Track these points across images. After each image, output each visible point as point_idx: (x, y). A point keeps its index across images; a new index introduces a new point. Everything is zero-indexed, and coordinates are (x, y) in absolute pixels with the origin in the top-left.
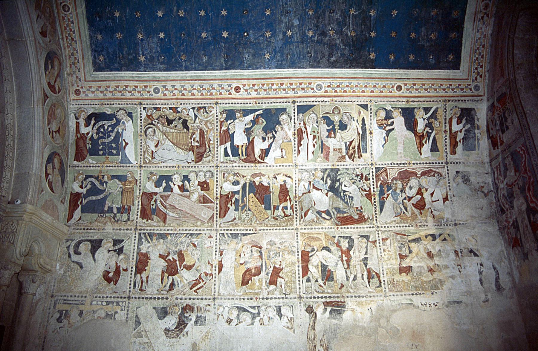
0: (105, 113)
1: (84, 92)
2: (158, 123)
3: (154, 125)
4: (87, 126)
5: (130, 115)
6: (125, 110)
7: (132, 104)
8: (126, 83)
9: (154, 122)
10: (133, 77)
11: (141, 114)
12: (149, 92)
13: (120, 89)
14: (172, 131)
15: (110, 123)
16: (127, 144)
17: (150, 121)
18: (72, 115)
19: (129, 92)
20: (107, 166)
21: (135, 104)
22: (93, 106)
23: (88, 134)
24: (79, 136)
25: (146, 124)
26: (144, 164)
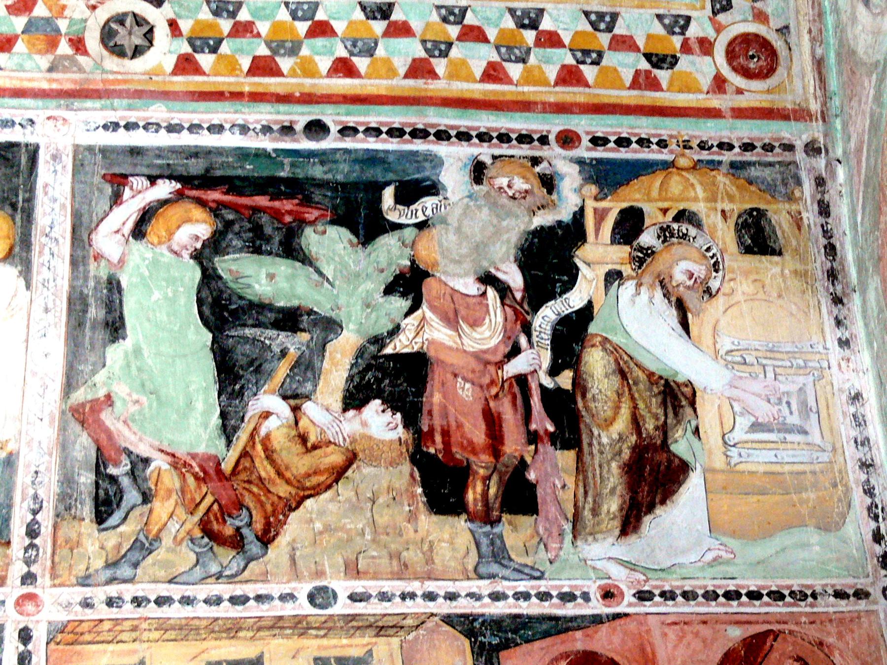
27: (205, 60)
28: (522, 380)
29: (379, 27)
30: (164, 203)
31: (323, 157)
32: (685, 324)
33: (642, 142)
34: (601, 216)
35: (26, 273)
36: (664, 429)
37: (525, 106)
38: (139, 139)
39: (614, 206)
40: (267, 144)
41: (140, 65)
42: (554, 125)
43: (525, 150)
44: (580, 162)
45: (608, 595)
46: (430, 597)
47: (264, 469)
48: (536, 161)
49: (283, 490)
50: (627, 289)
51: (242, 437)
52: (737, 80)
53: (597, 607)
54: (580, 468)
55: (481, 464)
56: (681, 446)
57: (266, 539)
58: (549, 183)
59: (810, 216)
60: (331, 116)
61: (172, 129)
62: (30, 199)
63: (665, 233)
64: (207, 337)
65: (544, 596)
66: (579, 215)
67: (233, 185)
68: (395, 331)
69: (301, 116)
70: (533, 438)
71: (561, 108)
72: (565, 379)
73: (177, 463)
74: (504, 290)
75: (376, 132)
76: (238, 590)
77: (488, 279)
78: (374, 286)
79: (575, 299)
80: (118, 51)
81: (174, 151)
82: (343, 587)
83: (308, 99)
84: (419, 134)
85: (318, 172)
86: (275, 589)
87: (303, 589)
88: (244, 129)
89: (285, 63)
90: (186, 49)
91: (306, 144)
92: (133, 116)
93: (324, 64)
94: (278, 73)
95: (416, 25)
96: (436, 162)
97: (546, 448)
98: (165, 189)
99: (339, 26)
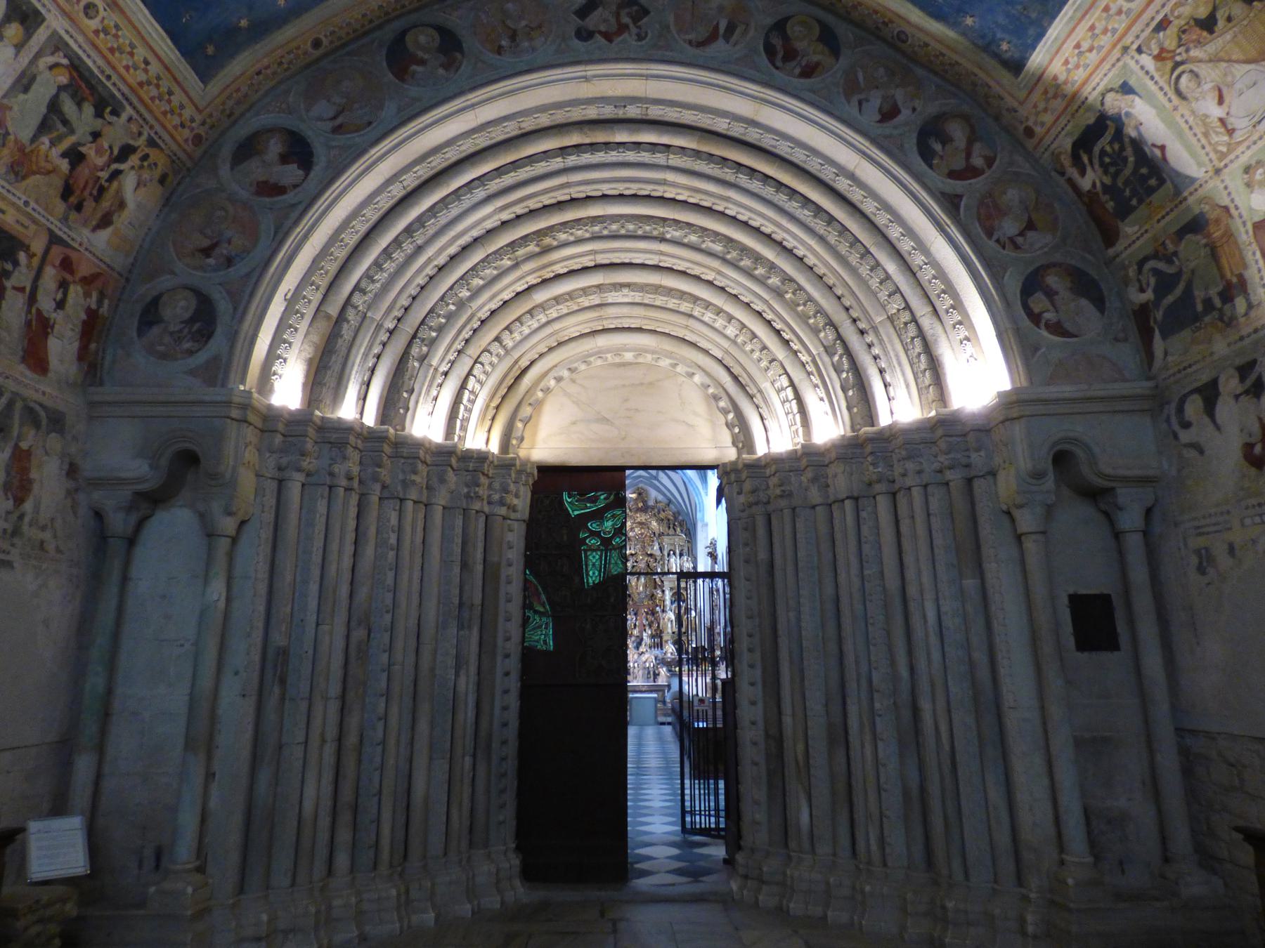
0: (1088, 127)
1: (1036, 123)
2: (1187, 51)
3: (1182, 63)
4: (1083, 173)
5: (1126, 89)
6: (1111, 90)
7: (1113, 65)
8: (1071, 43)
9: (1178, 58)
10: (1071, 18)
11: (1142, 68)
12: (1120, 12)
13: (1073, 61)
14: (1228, 37)
15: (1108, 136)
16: (1163, 148)
17: (1170, 64)
18: (1053, 174)
19: (1090, 50)
20: (1159, 221)
21: (1118, 60)
22: (1063, 133)
23: (1094, 185)
24: (1086, 199)
25: (1167, 76)
26: (1220, 160)
27: (102, 35)
28: (99, 178)
29: (143, 66)
30: (63, 65)
31: (105, 87)
32: (136, 189)
33: (163, 141)
34: (143, 150)
35: (16, 55)
36: (114, 211)
37: (150, 111)
38: (71, 42)
39: (147, 150)
40: (96, 71)
41: (86, 21)
42: (152, 122)
43: (141, 122)
44: (149, 135)
45: (80, 245)
46: (48, 220)
47: (34, 159)
48: (142, 127)
49: (34, 168)
50: (133, 172)
51: (34, 146)
52: (190, 142)
53: (76, 245)
54: (95, 209)
55: (78, 193)
56: (115, 218)
57: (24, 178)
58: (140, 134)
59: (175, 183)
60: (114, 78)
61: (80, 47)
62: (33, 33)
63: (149, 166)
64: (44, 110)
65: (69, 236)
66: (139, 147)
67: (81, 75)
68: (84, 145)
69: (109, 71)
70: (91, 194)
71: (157, 119)
72: (106, 185)
73: (16, 141)
74: (112, 153)
75: (119, 90)
76: (10, 188)
77: (111, 148)
78: (89, 129)
79: (122, 167)
80: (86, 14)
81: (76, 54)
82: (32, 204)
83: (114, 68)
84: (127, 99)
85: (100, 89)
86: (18, 194)
87: (24, 198)
88: (94, 62)
89: (117, 54)
90: (100, 28)
91: (103, 79)
92: (75, 34)
93: (124, 63)
94: (113, 55)
95: (150, 74)
96: (123, 108)
97: (92, 199)
98: (65, 61)
99: (136, 58)
